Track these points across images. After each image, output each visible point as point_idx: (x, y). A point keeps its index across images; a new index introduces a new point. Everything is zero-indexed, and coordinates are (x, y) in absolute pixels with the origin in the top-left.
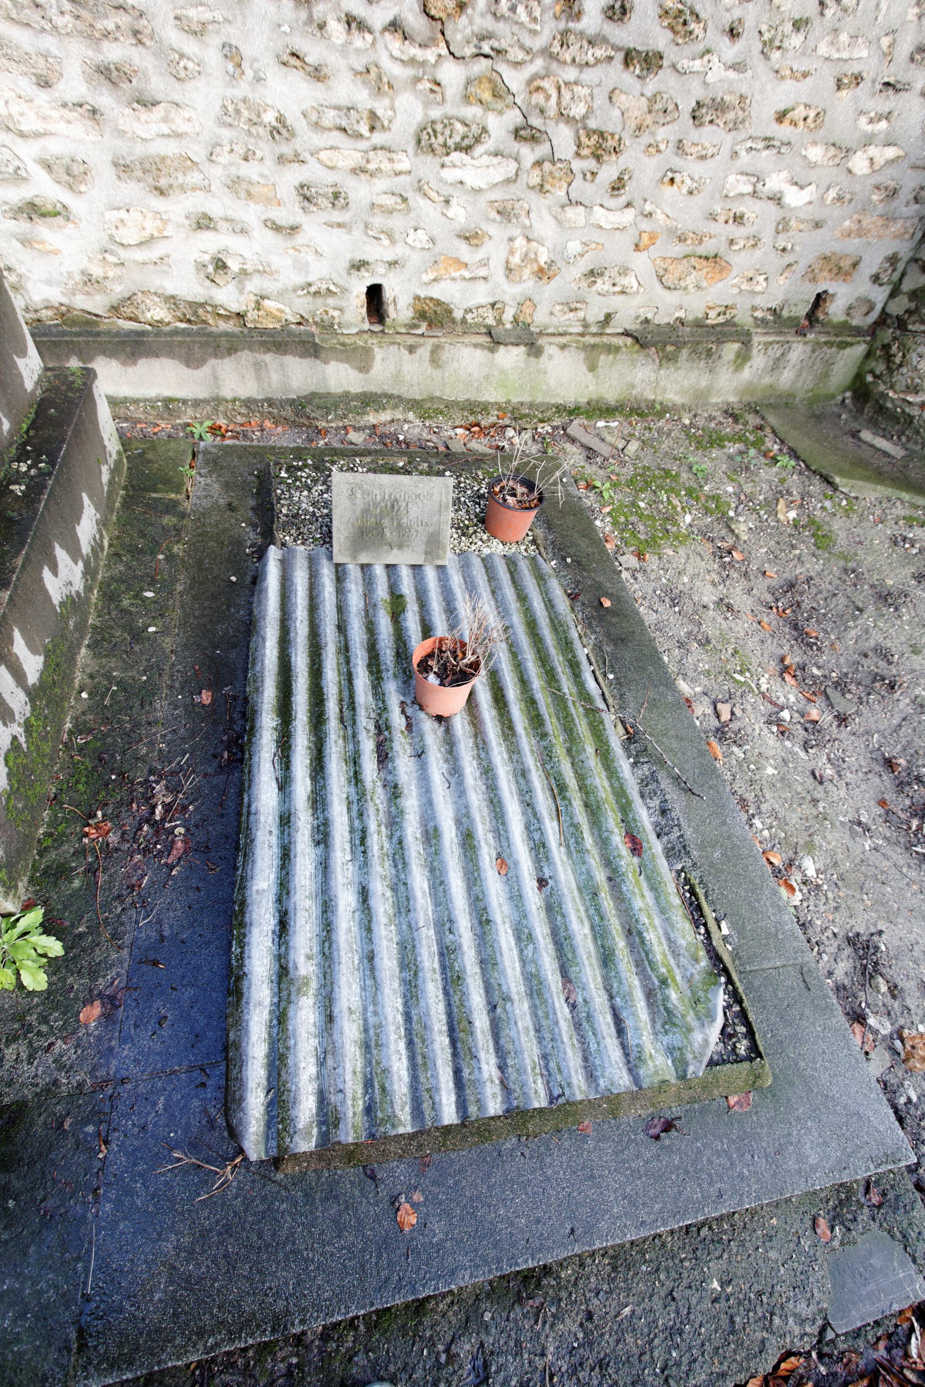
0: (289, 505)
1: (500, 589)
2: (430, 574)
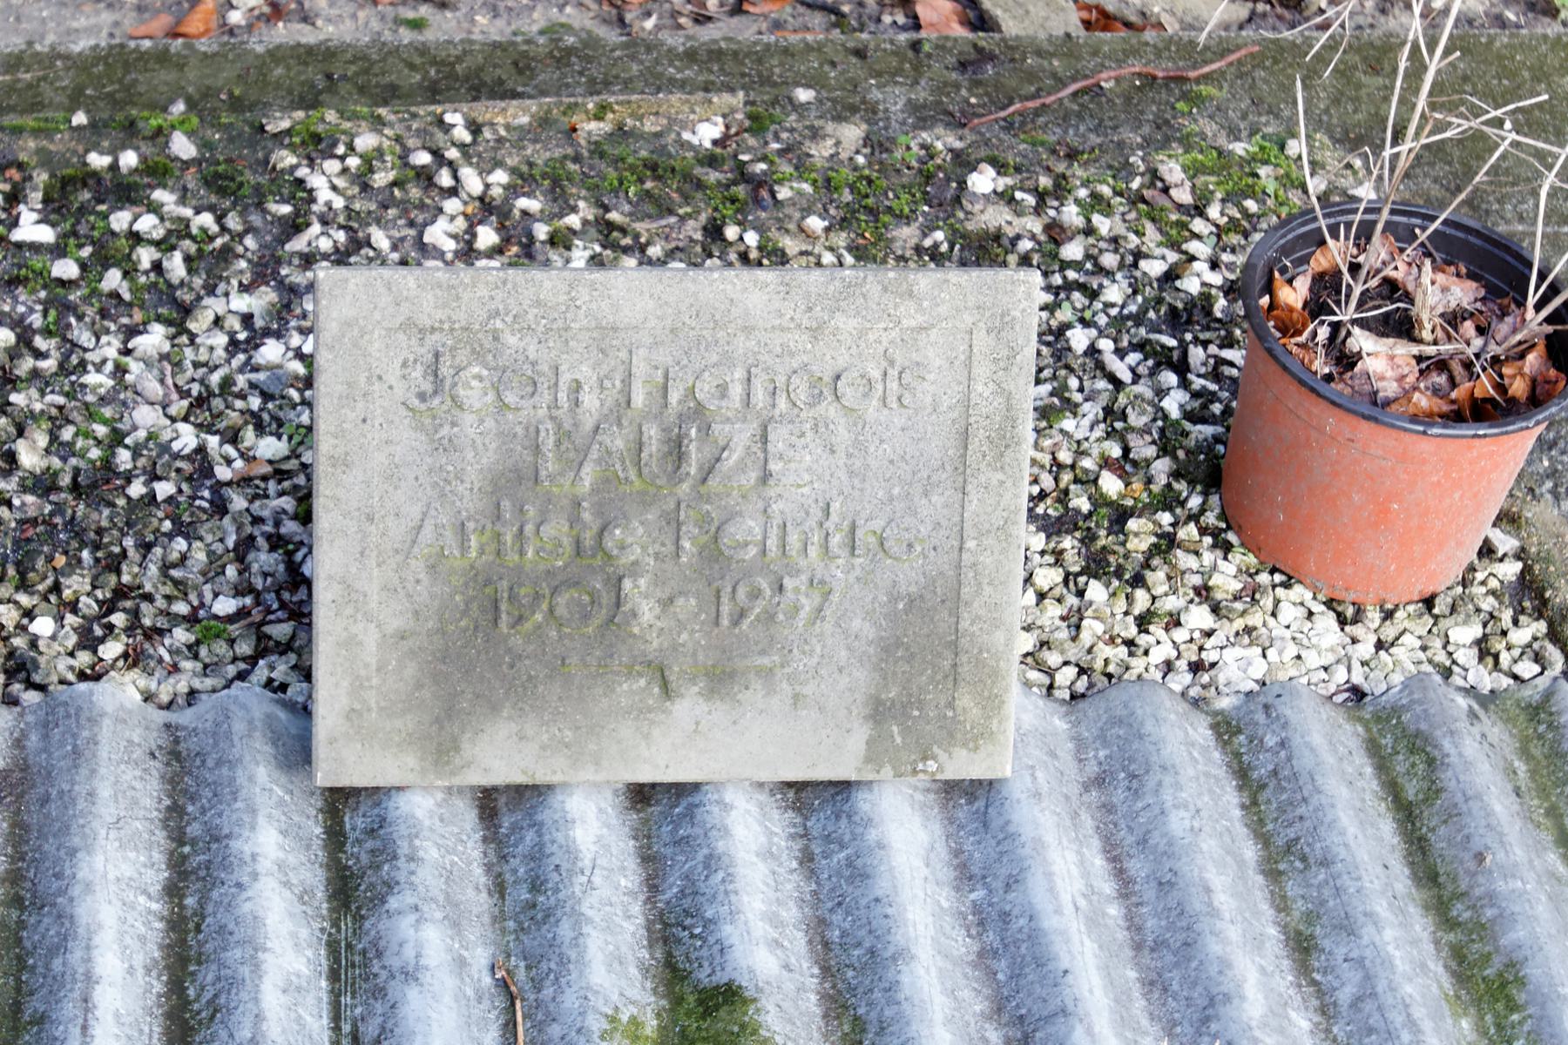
0: (59, 418)
1: (1347, 927)
2: (906, 839)
